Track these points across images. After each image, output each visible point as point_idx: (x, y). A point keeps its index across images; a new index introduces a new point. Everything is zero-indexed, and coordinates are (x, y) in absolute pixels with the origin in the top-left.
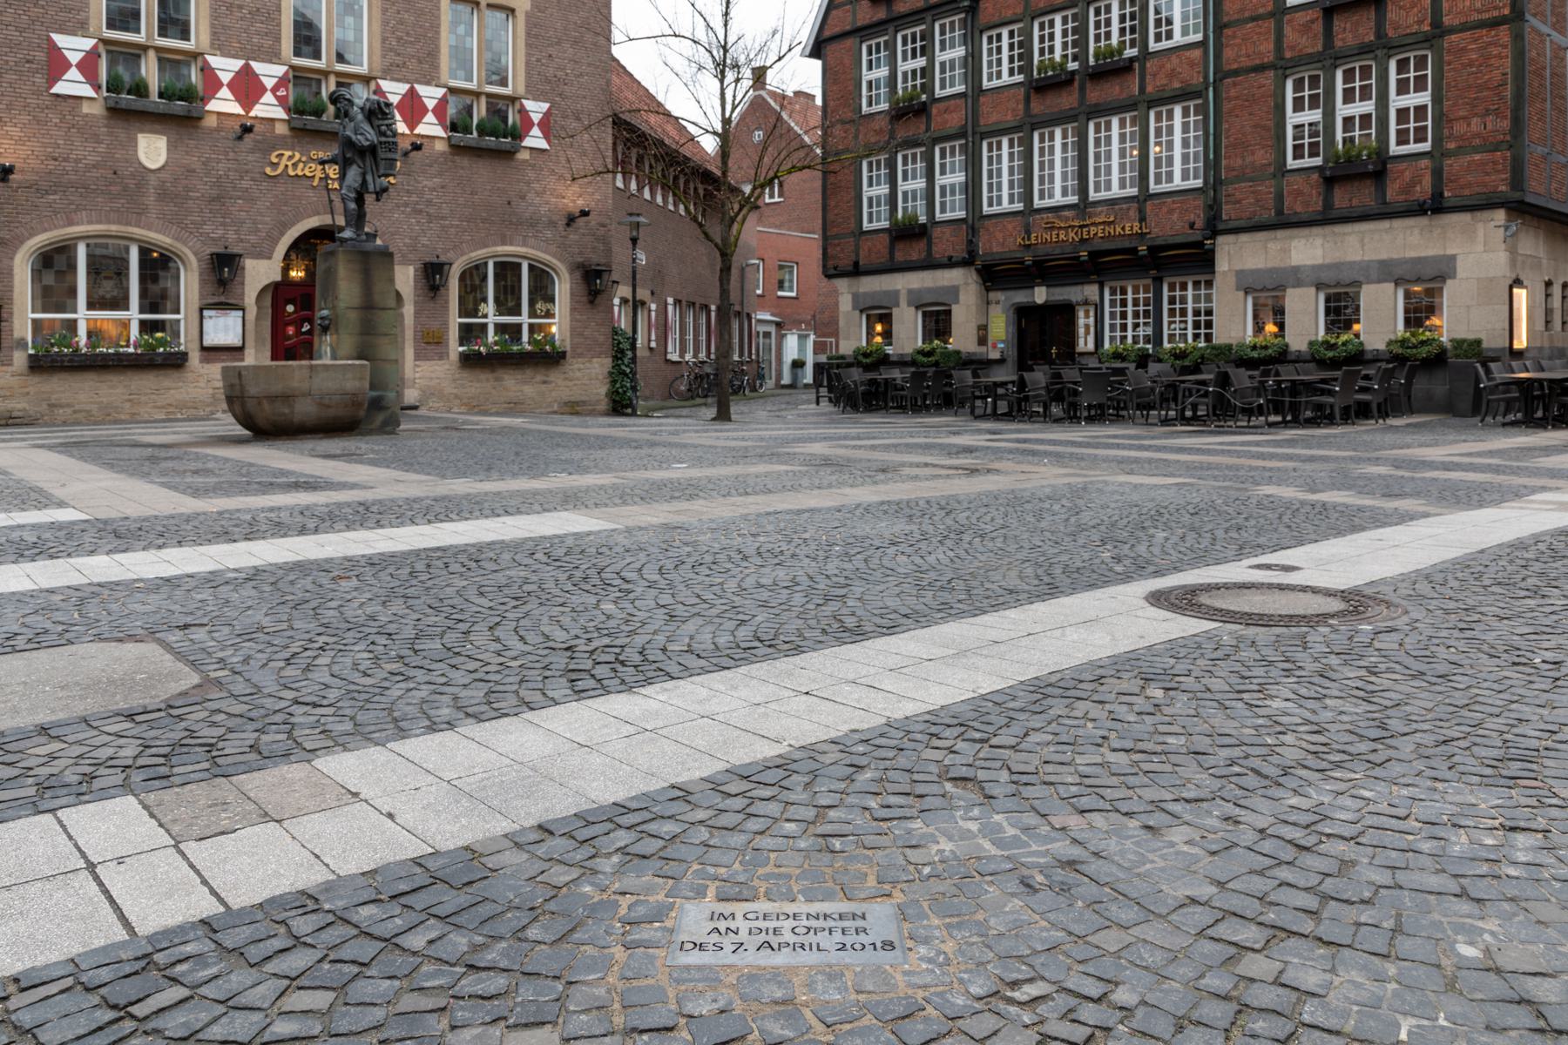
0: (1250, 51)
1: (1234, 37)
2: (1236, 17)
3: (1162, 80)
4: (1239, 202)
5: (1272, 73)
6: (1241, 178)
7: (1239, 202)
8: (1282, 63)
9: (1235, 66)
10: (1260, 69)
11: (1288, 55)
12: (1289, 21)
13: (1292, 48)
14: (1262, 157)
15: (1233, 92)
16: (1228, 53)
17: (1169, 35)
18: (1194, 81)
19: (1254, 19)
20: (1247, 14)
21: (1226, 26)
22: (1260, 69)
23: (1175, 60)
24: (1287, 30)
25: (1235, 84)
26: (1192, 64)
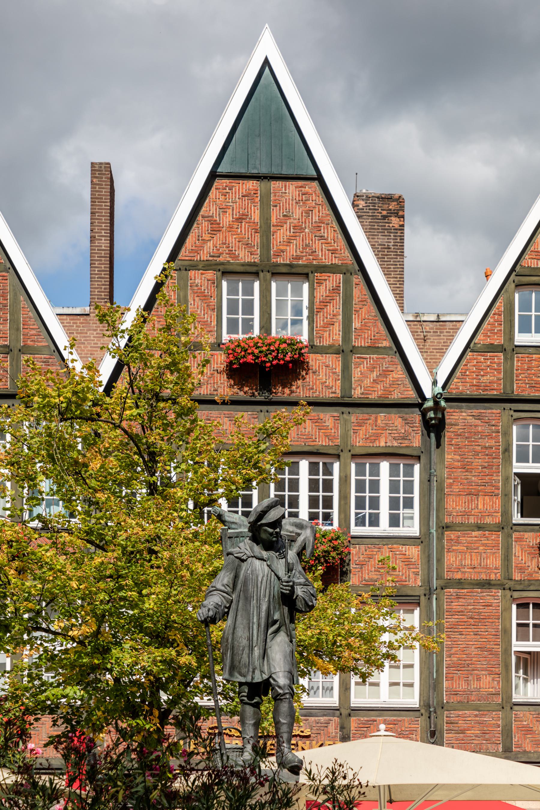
0: (475, 563)
1: (458, 542)
2: (459, 520)
3: (369, 573)
4: (463, 732)
5: (500, 593)
6: (464, 705)
7: (463, 732)
8: (510, 584)
9: (458, 576)
10: (486, 584)
11: (517, 576)
12: (518, 540)
13: (522, 570)
14: (488, 684)
15: (456, 606)
16: (450, 559)
17: (375, 521)
18: (411, 583)
19: (479, 527)
20: (472, 520)
21: (447, 527)
22: (486, 584)
23: (386, 552)
24: (516, 549)
25: (458, 597)
26: (408, 562)
